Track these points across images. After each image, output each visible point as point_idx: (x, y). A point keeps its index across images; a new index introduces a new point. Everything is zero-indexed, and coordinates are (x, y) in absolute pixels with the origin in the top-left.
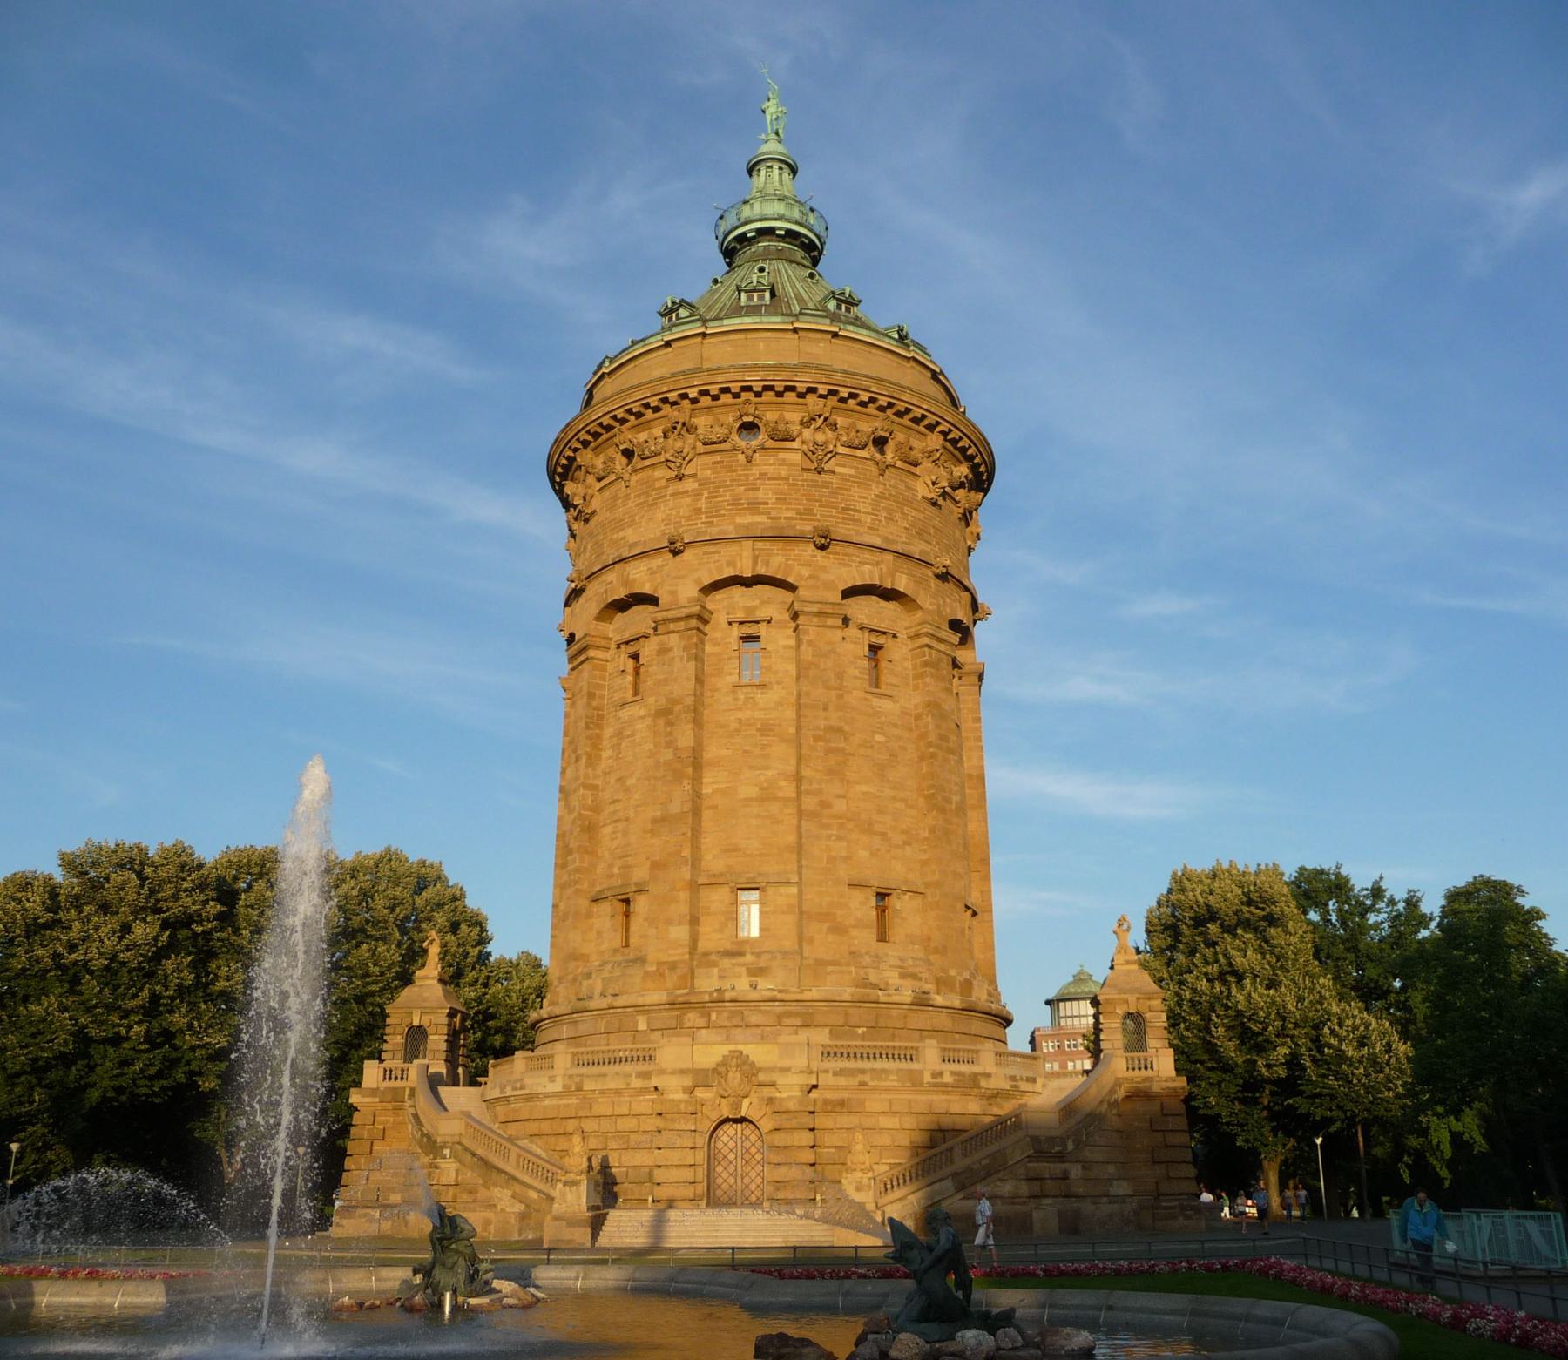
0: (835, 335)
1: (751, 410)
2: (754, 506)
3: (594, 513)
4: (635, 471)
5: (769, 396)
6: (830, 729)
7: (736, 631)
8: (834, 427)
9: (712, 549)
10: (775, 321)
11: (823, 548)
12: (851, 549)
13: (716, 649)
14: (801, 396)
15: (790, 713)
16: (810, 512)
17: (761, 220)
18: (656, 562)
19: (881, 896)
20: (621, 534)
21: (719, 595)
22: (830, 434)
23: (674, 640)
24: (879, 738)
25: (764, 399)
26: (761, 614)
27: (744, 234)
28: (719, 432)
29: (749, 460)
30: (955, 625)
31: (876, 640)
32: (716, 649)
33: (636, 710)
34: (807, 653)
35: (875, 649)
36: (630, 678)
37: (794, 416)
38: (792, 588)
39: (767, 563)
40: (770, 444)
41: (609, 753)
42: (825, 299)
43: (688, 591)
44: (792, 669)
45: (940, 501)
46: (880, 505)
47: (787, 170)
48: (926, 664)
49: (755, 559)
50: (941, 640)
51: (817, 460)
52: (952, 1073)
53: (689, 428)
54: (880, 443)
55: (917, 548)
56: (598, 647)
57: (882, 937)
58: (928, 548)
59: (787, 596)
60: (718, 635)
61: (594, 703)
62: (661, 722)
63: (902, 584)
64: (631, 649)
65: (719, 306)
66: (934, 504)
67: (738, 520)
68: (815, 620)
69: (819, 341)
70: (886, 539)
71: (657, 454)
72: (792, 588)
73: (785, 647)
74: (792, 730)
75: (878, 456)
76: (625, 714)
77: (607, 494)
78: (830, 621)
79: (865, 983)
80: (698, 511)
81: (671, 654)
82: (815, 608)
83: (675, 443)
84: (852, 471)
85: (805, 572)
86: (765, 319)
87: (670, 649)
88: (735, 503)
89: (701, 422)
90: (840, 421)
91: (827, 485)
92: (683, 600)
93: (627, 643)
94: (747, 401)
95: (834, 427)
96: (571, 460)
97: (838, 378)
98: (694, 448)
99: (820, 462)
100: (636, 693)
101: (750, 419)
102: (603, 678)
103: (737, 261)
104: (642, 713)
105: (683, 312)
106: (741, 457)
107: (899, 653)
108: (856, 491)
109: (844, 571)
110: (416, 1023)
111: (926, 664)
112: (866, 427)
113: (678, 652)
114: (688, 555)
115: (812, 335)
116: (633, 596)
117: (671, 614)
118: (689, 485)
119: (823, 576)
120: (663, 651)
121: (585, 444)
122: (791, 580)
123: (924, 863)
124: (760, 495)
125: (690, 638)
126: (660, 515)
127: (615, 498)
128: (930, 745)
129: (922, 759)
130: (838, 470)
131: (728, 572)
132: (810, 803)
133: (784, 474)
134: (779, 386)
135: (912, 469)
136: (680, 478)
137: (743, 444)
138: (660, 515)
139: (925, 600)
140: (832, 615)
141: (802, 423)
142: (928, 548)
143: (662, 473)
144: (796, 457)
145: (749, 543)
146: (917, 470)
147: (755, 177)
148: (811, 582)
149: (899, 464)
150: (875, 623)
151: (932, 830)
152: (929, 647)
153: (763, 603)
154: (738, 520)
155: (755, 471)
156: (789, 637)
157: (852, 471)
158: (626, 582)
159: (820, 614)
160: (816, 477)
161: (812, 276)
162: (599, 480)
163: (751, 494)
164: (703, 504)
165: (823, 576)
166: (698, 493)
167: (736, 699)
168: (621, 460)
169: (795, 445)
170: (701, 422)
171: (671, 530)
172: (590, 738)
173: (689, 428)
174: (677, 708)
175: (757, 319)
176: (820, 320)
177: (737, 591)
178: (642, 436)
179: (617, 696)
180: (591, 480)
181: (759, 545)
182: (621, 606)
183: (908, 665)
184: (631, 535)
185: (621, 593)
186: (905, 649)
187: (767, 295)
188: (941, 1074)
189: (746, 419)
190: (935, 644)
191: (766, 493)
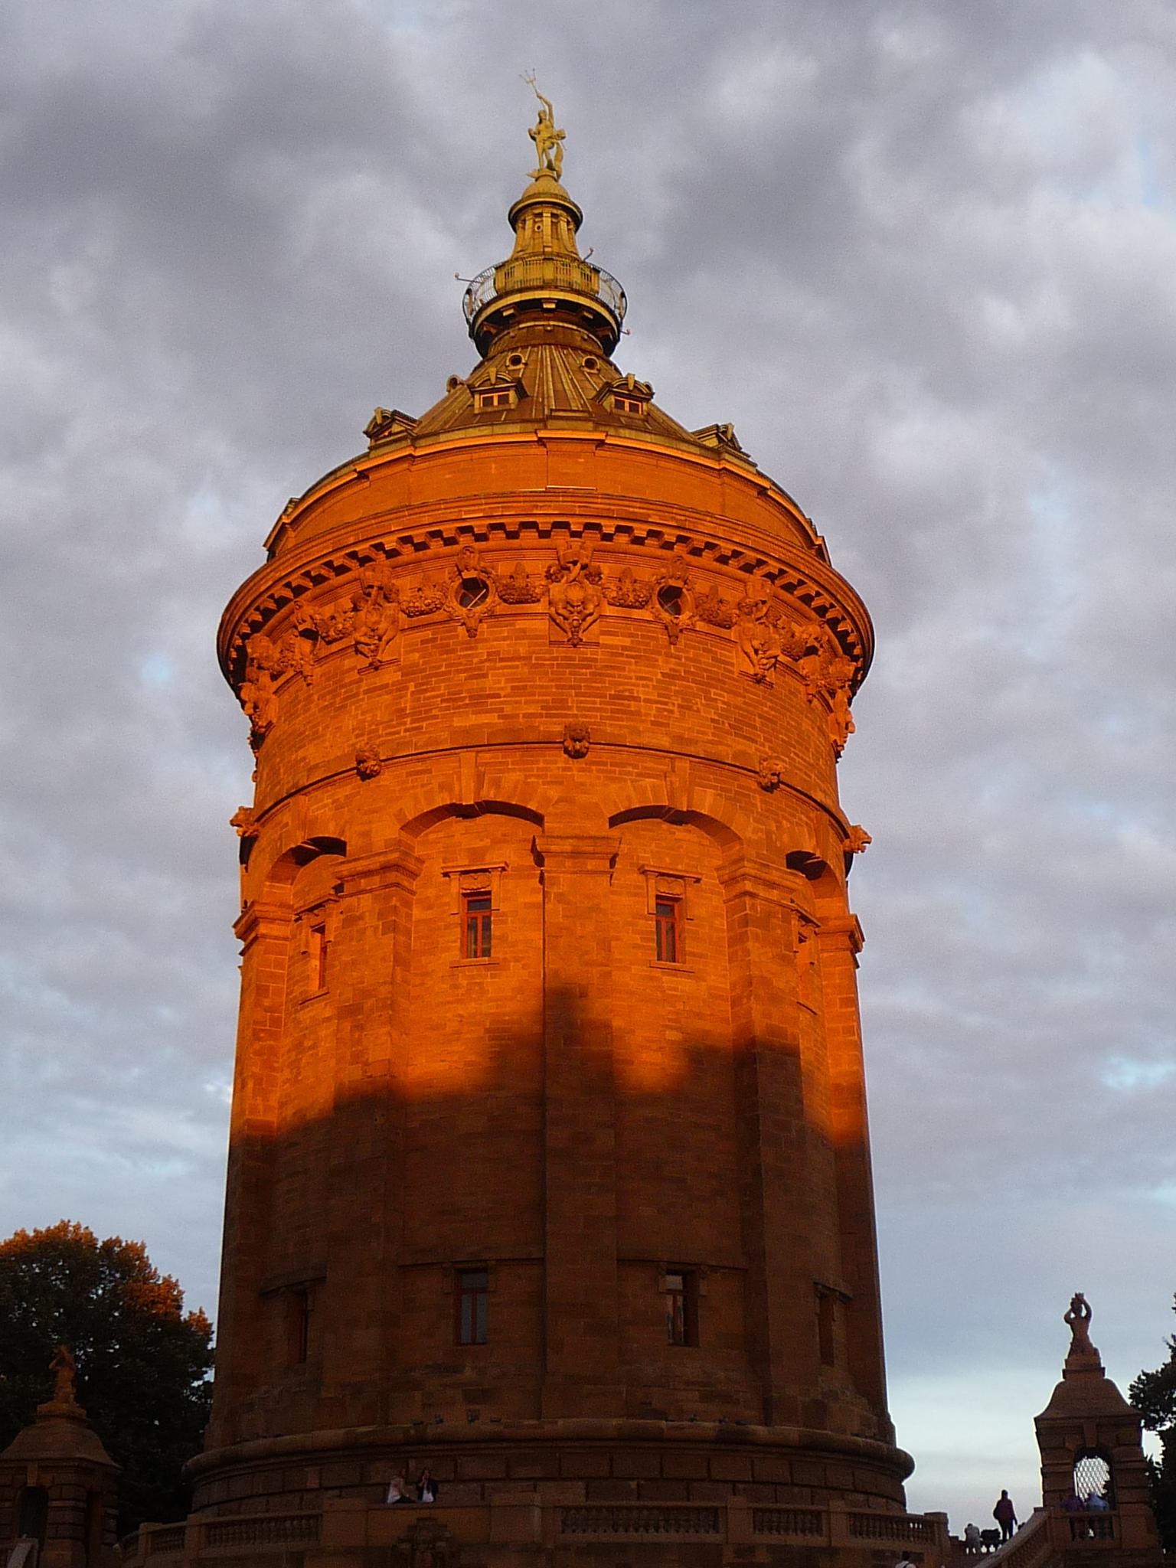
0: (601, 443)
1: (473, 563)
2: (479, 701)
3: (270, 723)
4: (318, 660)
5: (529, 537)
7: (455, 886)
8: (594, 576)
9: (420, 766)
10: (512, 433)
11: (577, 755)
12: (624, 756)
13: (428, 914)
14: (512, 535)
16: (562, 704)
17: (520, 291)
18: (343, 792)
20: (301, 754)
21: (435, 833)
22: (590, 589)
23: (366, 902)
25: (490, 544)
26: (493, 859)
27: (499, 312)
28: (431, 594)
29: (472, 633)
30: (798, 861)
31: (664, 889)
32: (428, 914)
33: (322, 1010)
34: (556, 912)
36: (316, 963)
37: (537, 565)
38: (537, 819)
39: (496, 783)
40: (501, 608)
41: (287, 1074)
42: (600, 396)
43: (386, 830)
44: (537, 936)
45: (771, 676)
46: (661, 690)
47: (564, 218)
49: (480, 779)
50: (772, 885)
51: (570, 628)
52: (771, 1548)
53: (388, 594)
54: (670, 597)
55: (730, 748)
56: (273, 920)
58: (751, 749)
59: (532, 829)
60: (431, 892)
61: (267, 1003)
62: (347, 1025)
63: (706, 802)
64: (315, 921)
65: (445, 416)
66: (759, 680)
68: (568, 863)
69: (578, 455)
70: (680, 739)
71: (344, 634)
72: (537, 819)
73: (532, 905)
75: (666, 617)
76: (306, 1015)
77: (286, 697)
78: (591, 865)
80: (401, 713)
81: (361, 924)
82: (567, 846)
83: (367, 615)
84: (627, 642)
85: (554, 793)
86: (497, 429)
87: (361, 918)
88: (453, 698)
89: (405, 584)
90: (606, 569)
91: (588, 663)
92: (379, 845)
93: (311, 910)
94: (467, 548)
95: (594, 576)
96: (242, 650)
97: (600, 505)
98: (395, 621)
99: (576, 629)
100: (321, 986)
101: (472, 574)
102: (279, 965)
103: (492, 352)
104: (328, 1012)
105: (396, 428)
106: (461, 630)
107: (707, 908)
108: (633, 669)
109: (614, 786)
110: (31, 1482)
112: (647, 574)
113: (370, 921)
114: (386, 779)
115: (566, 447)
116: (315, 841)
117: (361, 865)
118: (390, 676)
119: (582, 798)
120: (351, 920)
121: (256, 627)
122: (532, 806)
124: (489, 683)
125: (388, 898)
126: (350, 723)
127: (294, 702)
130: (603, 640)
131: (442, 800)
133: (523, 651)
134: (512, 523)
135: (724, 633)
136: (375, 667)
137: (462, 611)
138: (350, 723)
139: (746, 827)
140: (593, 855)
141: (549, 576)
142: (751, 749)
143: (351, 661)
144: (542, 626)
145: (469, 756)
146: (732, 634)
147: (520, 231)
148: (563, 807)
149: (700, 626)
150: (666, 864)
152: (753, 895)
153: (494, 842)
154: (457, 723)
155: (482, 650)
156: (533, 891)
157: (627, 642)
158: (305, 823)
159: (575, 854)
160: (571, 652)
161: (590, 364)
162: (274, 677)
163: (475, 684)
164: (407, 702)
165: (582, 798)
166: (401, 687)
167: (456, 987)
169: (540, 607)
170: (405, 584)
171: (361, 743)
172: (258, 1053)
173: (388, 594)
174: (371, 1002)
175: (486, 430)
176: (578, 424)
177: (457, 827)
178: (328, 610)
179: (297, 990)
180: (265, 678)
181: (487, 757)
182: (301, 856)
183: (721, 923)
184: (312, 753)
185: (298, 839)
186: (717, 901)
187: (512, 394)
188: (752, 1549)
189: (466, 575)
190: (762, 891)
191: (496, 681)
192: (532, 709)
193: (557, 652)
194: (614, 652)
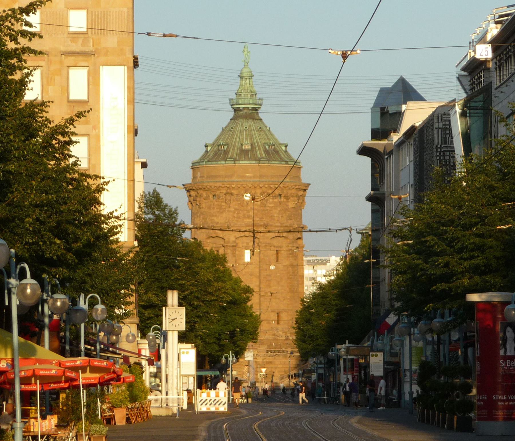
6: (267, 275)
15: (257, 270)
16: (262, 218)
19: (278, 313)
20: (213, 218)
24: (278, 274)
35: (277, 252)
48: (290, 254)
57: (278, 323)
67: (245, 221)
74: (258, 274)
79: (274, 335)
80: (234, 217)
82: (264, 245)
88: (244, 216)
91: (267, 210)
97: (271, 183)
107: (284, 253)
108: (274, 210)
111: (290, 254)
123: (288, 305)
126: (224, 215)
128: (290, 275)
129: (288, 278)
132: (262, 294)
151: (290, 297)
163: (248, 214)
164: (236, 215)
168: (211, 196)
183: (285, 253)
192: (258, 219)
193: (262, 208)
194: (272, 208)
